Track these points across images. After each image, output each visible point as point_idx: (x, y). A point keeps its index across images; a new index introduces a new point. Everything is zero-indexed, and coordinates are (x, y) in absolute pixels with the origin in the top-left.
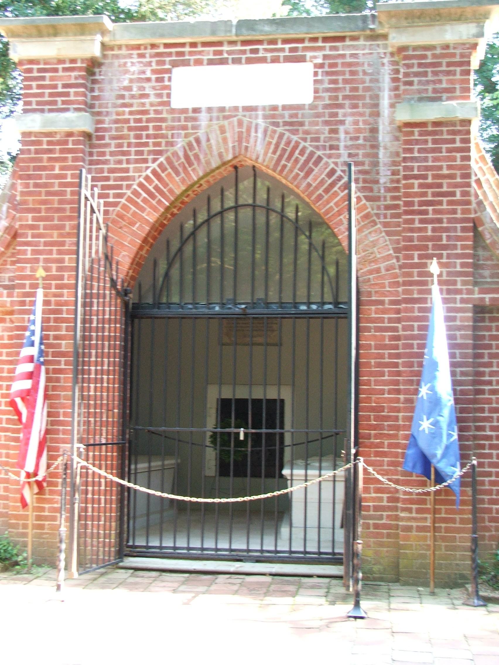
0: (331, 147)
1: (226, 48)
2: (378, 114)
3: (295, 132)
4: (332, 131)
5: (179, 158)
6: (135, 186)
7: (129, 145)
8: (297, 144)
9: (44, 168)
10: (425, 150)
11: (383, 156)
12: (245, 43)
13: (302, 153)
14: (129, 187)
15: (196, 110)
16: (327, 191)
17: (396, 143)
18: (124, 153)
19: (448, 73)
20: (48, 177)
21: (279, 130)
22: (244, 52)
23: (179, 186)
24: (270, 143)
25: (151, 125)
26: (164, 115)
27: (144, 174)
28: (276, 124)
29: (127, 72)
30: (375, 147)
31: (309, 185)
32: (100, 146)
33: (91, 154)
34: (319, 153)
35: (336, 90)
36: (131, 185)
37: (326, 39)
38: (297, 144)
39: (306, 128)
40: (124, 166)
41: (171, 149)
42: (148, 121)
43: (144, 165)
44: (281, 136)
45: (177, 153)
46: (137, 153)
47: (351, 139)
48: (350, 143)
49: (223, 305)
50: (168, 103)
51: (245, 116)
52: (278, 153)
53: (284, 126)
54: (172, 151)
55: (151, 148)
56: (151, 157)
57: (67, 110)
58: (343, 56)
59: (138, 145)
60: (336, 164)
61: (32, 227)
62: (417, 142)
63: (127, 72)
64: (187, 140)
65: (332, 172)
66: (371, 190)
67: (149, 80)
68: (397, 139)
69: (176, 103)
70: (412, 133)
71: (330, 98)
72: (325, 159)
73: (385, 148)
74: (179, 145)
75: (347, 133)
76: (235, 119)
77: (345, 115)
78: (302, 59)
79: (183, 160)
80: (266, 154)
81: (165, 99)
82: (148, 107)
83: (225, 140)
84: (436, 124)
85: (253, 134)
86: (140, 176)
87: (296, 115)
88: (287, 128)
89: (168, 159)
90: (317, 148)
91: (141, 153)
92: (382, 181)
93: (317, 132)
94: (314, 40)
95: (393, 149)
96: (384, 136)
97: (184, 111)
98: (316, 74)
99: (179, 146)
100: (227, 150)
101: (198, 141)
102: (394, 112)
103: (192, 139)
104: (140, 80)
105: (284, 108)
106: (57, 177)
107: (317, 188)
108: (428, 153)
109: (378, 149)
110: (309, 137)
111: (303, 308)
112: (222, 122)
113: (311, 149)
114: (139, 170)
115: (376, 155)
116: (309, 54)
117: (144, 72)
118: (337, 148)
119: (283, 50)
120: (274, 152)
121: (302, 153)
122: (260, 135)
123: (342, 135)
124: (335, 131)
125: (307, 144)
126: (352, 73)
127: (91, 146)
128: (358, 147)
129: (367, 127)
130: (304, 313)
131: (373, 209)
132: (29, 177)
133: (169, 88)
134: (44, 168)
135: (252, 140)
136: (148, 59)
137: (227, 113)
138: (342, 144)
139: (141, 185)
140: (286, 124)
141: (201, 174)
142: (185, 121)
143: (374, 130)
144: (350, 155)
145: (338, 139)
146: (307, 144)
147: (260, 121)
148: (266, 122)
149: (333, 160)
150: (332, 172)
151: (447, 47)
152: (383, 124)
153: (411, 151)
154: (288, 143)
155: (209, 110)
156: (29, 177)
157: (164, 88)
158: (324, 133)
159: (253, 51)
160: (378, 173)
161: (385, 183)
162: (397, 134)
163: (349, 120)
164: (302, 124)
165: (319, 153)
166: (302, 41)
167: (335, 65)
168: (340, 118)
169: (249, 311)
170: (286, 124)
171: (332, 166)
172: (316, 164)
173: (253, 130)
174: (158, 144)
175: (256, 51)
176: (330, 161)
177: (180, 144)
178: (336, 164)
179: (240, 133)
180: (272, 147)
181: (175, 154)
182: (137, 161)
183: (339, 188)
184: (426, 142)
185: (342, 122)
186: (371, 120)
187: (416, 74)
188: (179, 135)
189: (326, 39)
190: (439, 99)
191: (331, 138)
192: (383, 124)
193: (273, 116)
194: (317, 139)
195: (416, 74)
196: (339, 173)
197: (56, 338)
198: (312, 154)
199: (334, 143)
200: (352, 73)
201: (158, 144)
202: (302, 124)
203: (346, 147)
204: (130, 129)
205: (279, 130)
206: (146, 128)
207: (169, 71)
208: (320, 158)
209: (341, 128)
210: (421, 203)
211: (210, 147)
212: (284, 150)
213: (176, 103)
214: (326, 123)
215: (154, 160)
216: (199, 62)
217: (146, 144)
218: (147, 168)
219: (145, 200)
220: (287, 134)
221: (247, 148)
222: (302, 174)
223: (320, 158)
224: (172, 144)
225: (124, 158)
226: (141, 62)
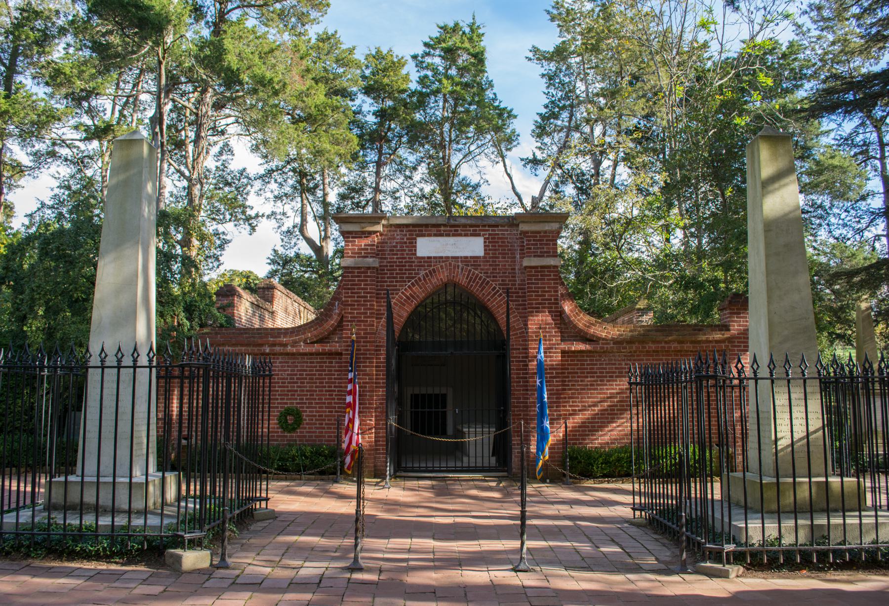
1: (442, 228)
3: (476, 269)
9: (356, 285)
12: (452, 226)
13: (480, 279)
14: (397, 294)
15: (429, 258)
16: (492, 297)
18: (394, 278)
19: (547, 244)
20: (358, 289)
28: (468, 265)
29: (394, 239)
33: (378, 278)
35: (495, 250)
37: (489, 226)
38: (477, 275)
44: (470, 271)
57: (367, 257)
61: (350, 313)
62: (534, 276)
63: (394, 239)
65: (495, 288)
67: (406, 243)
69: (419, 254)
78: (479, 235)
84: (542, 267)
94: (485, 226)
98: (485, 242)
104: (401, 243)
105: (471, 257)
106: (363, 289)
107: (488, 295)
114: (402, 286)
121: (480, 279)
126: (502, 242)
128: (506, 277)
132: (349, 289)
133: (415, 247)
134: (356, 285)
139: (403, 293)
150: (495, 288)
151: (545, 232)
153: (531, 279)
155: (435, 258)
156: (349, 289)
157: (413, 246)
164: (480, 265)
166: (478, 226)
172: (487, 284)
181: (419, 279)
182: (400, 282)
187: (532, 244)
189: (489, 226)
190: (543, 256)
195: (532, 244)
197: (364, 367)
198: (485, 280)
200: (502, 242)
202: (480, 265)
204: (397, 266)
208: (488, 282)
210: (536, 304)
213: (419, 254)
214: (490, 265)
216: (430, 235)
223: (488, 282)
224: (418, 274)
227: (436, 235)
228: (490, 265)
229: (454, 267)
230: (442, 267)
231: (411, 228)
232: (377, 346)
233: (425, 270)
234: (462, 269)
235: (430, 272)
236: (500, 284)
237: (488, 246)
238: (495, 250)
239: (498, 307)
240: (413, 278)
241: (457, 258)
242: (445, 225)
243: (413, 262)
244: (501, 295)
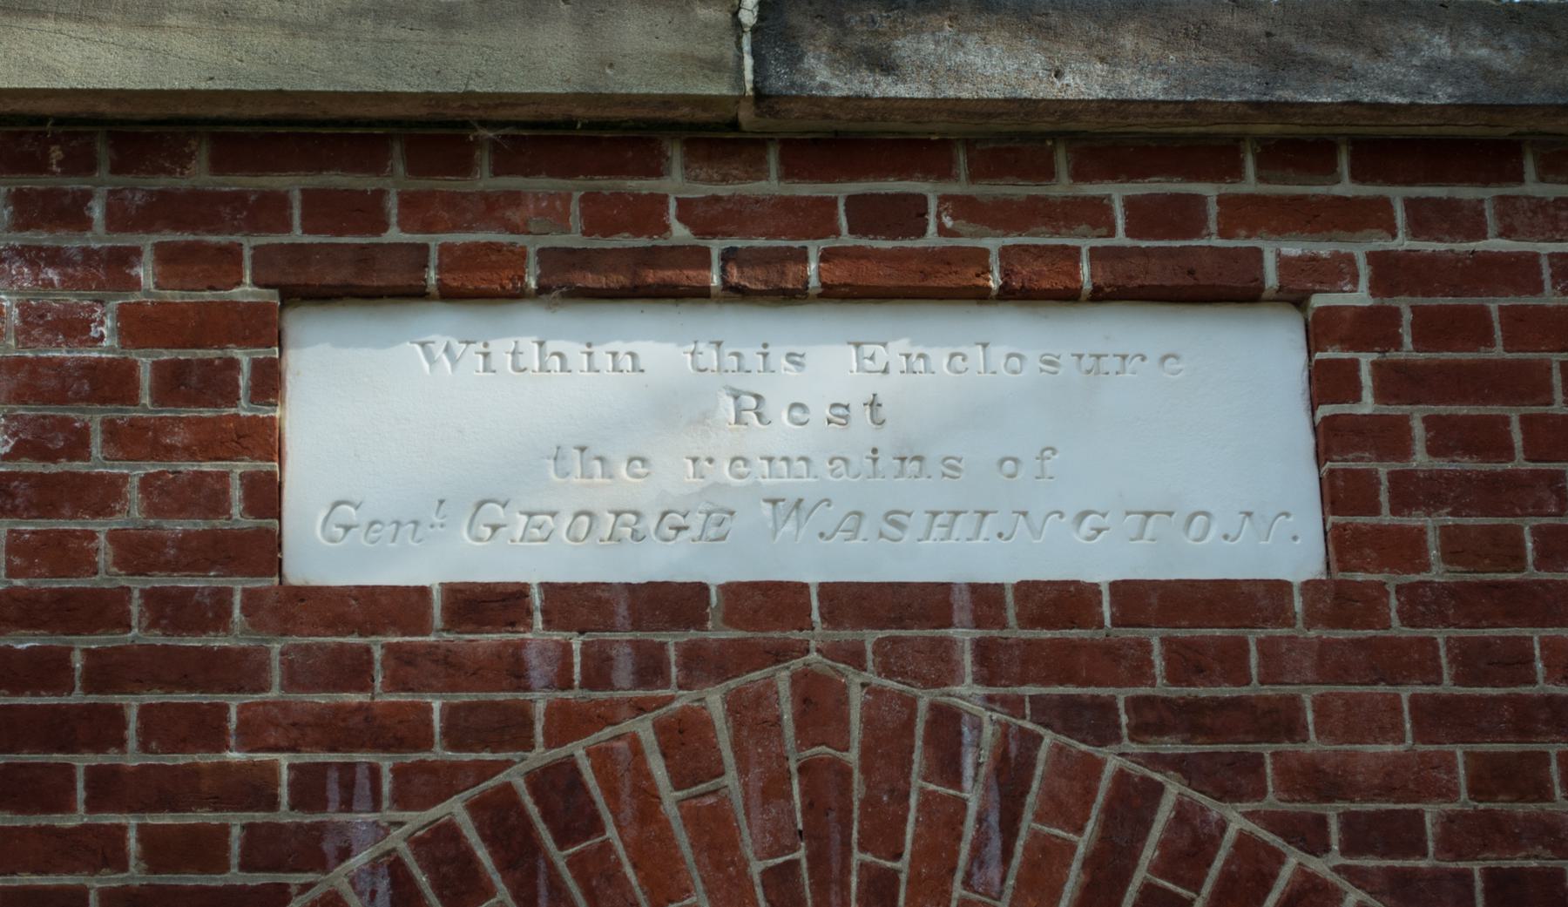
3: (1235, 779)
4: (1493, 777)
22: (817, 218)
25: (132, 704)
26: (233, 638)
28: (1093, 721)
35: (1496, 493)
39: (1313, 745)
42: (105, 672)
44: (1133, 802)
50: (264, 550)
51: (855, 657)
53: (1138, 732)
58: (1521, 271)
64: (416, 820)
67: (111, 382)
69: (317, 553)
71: (1456, 547)
74: (360, 860)
76: (782, 677)
81: (238, 517)
82: (106, 575)
87: (1231, 661)
88: (1170, 746)
93: (1392, 780)
97: (398, 606)
98: (1327, 383)
99: (360, 860)
110: (1333, 812)
112: (683, 699)
116: (1276, 252)
117: (75, 328)
119: (1096, 214)
136: (98, 237)
137: (716, 632)
140: (1153, 718)
142: (396, 683)
147: (967, 693)
148: (1013, 705)
155: (570, 603)
158: (1450, 794)
159: (868, 216)
167: (1474, 328)
170: (1153, 718)
175: (908, 215)
193: (1062, 663)
202: (1280, 721)
206: (103, 728)
207: (264, 329)
213: (317, 553)
214: (1437, 718)
216: (481, 285)
220: (1174, 789)
226: (55, 257)
227: (576, 283)
228: (1437, 718)
229: (888, 744)
230: (685, 741)
231: (199, 176)
233: (418, 787)
234: (1010, 776)
235: (499, 816)
237: (1387, 437)
238: (1496, 493)
241: (924, 603)
242: (713, 135)
243: (238, 671)
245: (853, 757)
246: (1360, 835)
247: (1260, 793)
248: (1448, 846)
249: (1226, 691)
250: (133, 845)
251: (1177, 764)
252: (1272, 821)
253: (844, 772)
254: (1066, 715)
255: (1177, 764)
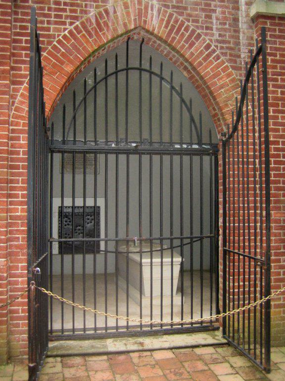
0: (207, 28)
2: (238, 9)
3: (181, 14)
4: (206, 16)
5: (91, 24)
6: (55, 43)
7: (50, 9)
8: (182, 24)
10: (275, 36)
11: (243, 39)
13: (187, 29)
14: (50, 43)
16: (205, 59)
17: (251, 31)
18: (45, 15)
21: (169, 11)
23: (91, 45)
24: (162, 20)
27: (63, 34)
28: (167, 7)
30: (237, 31)
31: (192, 54)
32: (24, 7)
33: (16, 13)
34: (199, 31)
36: (54, 41)
38: (182, 24)
39: (189, 12)
40: (46, 25)
41: (85, 17)
43: (63, 27)
44: (171, 16)
45: (90, 20)
46: (56, 16)
47: (220, 24)
48: (220, 27)
49: (117, 143)
52: (169, 28)
54: (85, 18)
55: (68, 14)
56: (68, 21)
59: (56, 10)
60: (211, 40)
64: (97, 10)
66: (235, 62)
68: (251, 27)
70: (266, 23)
72: (203, 36)
73: (244, 33)
75: (217, 19)
77: (215, 6)
79: (95, 25)
80: (160, 27)
83: (128, 14)
85: (150, 12)
86: (59, 36)
88: (175, 10)
89: (82, 24)
90: (197, 27)
91: (61, 17)
92: (242, 56)
93: (197, 16)
95: (249, 35)
96: (243, 25)
99: (92, 14)
100: (130, 21)
101: (107, 11)
102: (249, 8)
103: (102, 10)
107: (198, 57)
108: (277, 38)
109: (239, 33)
110: (191, 19)
111: (177, 146)
113: (192, 27)
114: (59, 30)
115: (238, 38)
118: (211, 29)
120: (166, 27)
121: (187, 29)
122: (155, 13)
123: (214, 21)
124: (210, 17)
125: (190, 24)
127: (16, 6)
128: (225, 30)
129: (231, 17)
130: (178, 150)
131: (237, 76)
135: (149, 16)
138: (214, 27)
139: (59, 42)
140: (174, 7)
141: (110, 38)
143: (236, 20)
144: (220, 35)
145: (212, 23)
146: (190, 24)
148: (160, 4)
149: (208, 37)
150: (208, 47)
152: (242, 16)
154: (176, 21)
160: (239, 50)
161: (244, 58)
162: (251, 24)
163: (219, 10)
164: (186, 8)
165: (199, 31)
168: (212, 8)
169: (139, 148)
170: (174, 7)
171: (208, 41)
173: (150, 9)
174: (75, 11)
176: (207, 38)
177: (92, 13)
178: (211, 40)
179: (140, 10)
180: (165, 23)
181: (88, 20)
182: (56, 23)
183: (214, 58)
184: (275, 30)
185: (214, 11)
186: (233, 12)
188: (91, 6)
191: (206, 22)
192: (242, 16)
194: (197, 21)
196: (213, 47)
198: (193, 32)
199: (209, 25)
201: (75, 11)
202: (186, 8)
203: (217, 29)
205: (169, 11)
209: (214, 15)
211: (116, 18)
212: (173, 27)
214: (203, 10)
215: (71, 24)
217: (65, 10)
218: (65, 29)
219: (63, 55)
220: (175, 15)
221: (145, 22)
222: (187, 46)
223: (199, 36)
224: (86, 12)
225: (46, 19)
232: (13, 131)
234: (159, 11)
236: (217, 41)
239: (215, 76)
240: (76, 18)
244: (218, 58)
245: (143, 8)
246: (193, 21)
247: (184, 16)
248: (202, 23)
249: (181, 5)
250: (68, 10)
251: (176, 12)
252: (184, 19)
253: (142, 9)
254: (165, 6)
255: (176, 12)
